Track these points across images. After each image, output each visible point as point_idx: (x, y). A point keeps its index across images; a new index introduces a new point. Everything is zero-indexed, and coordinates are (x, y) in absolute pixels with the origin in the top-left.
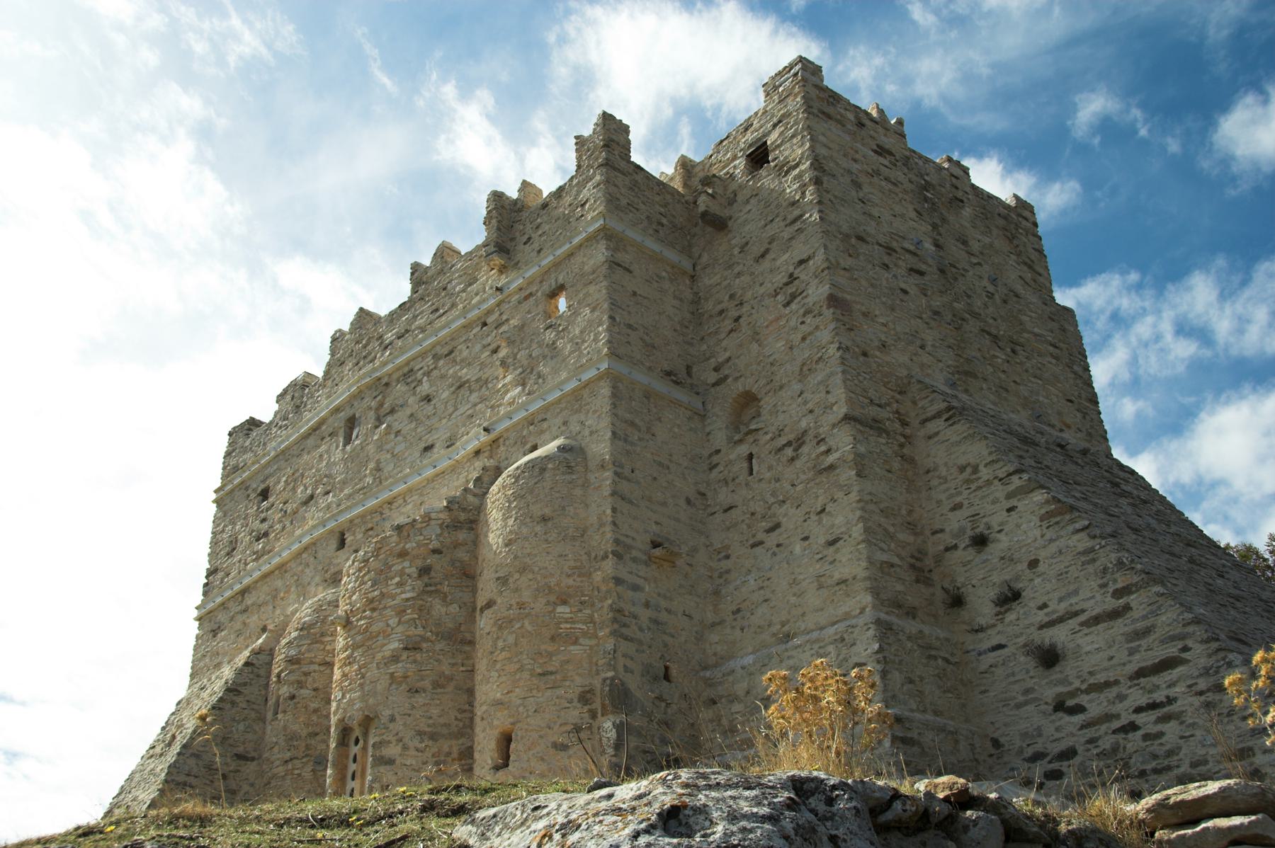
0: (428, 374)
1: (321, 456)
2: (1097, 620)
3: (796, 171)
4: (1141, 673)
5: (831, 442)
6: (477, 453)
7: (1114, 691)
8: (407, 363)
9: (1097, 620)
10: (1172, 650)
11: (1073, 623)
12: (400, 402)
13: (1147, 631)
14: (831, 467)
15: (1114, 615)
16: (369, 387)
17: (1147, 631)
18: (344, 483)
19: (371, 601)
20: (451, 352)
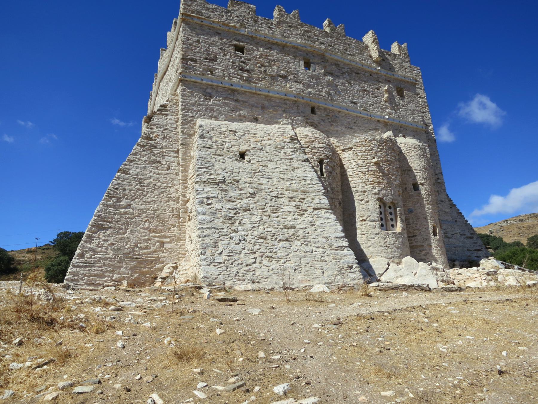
0: (349, 74)
1: (288, 62)
2: (468, 237)
3: (423, 100)
4: (475, 250)
5: (439, 177)
6: (378, 121)
7: (471, 252)
8: (337, 61)
9: (468, 237)
10: (480, 248)
11: (464, 236)
12: (336, 74)
13: (476, 243)
14: (439, 183)
15: (471, 238)
16: (319, 55)
17: (476, 243)
18: (308, 86)
19: (388, 160)
20: (358, 74)
